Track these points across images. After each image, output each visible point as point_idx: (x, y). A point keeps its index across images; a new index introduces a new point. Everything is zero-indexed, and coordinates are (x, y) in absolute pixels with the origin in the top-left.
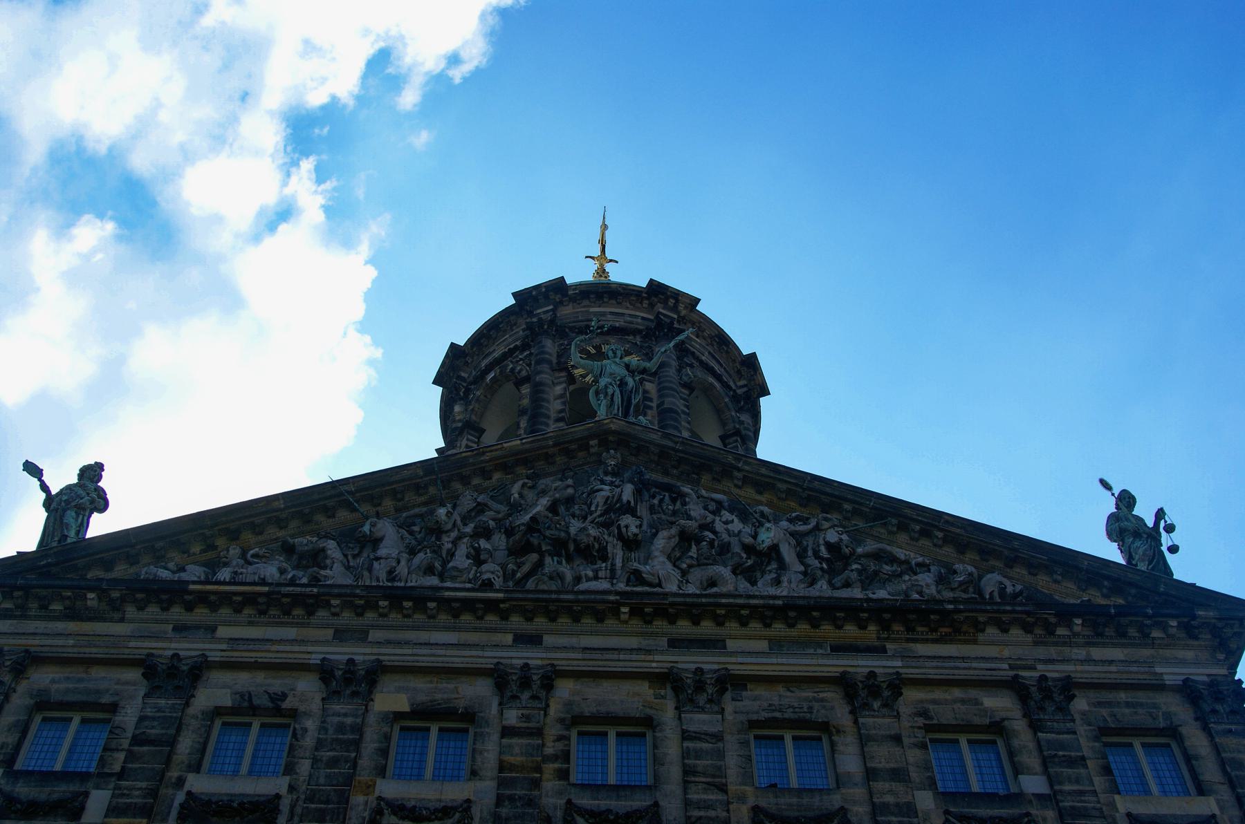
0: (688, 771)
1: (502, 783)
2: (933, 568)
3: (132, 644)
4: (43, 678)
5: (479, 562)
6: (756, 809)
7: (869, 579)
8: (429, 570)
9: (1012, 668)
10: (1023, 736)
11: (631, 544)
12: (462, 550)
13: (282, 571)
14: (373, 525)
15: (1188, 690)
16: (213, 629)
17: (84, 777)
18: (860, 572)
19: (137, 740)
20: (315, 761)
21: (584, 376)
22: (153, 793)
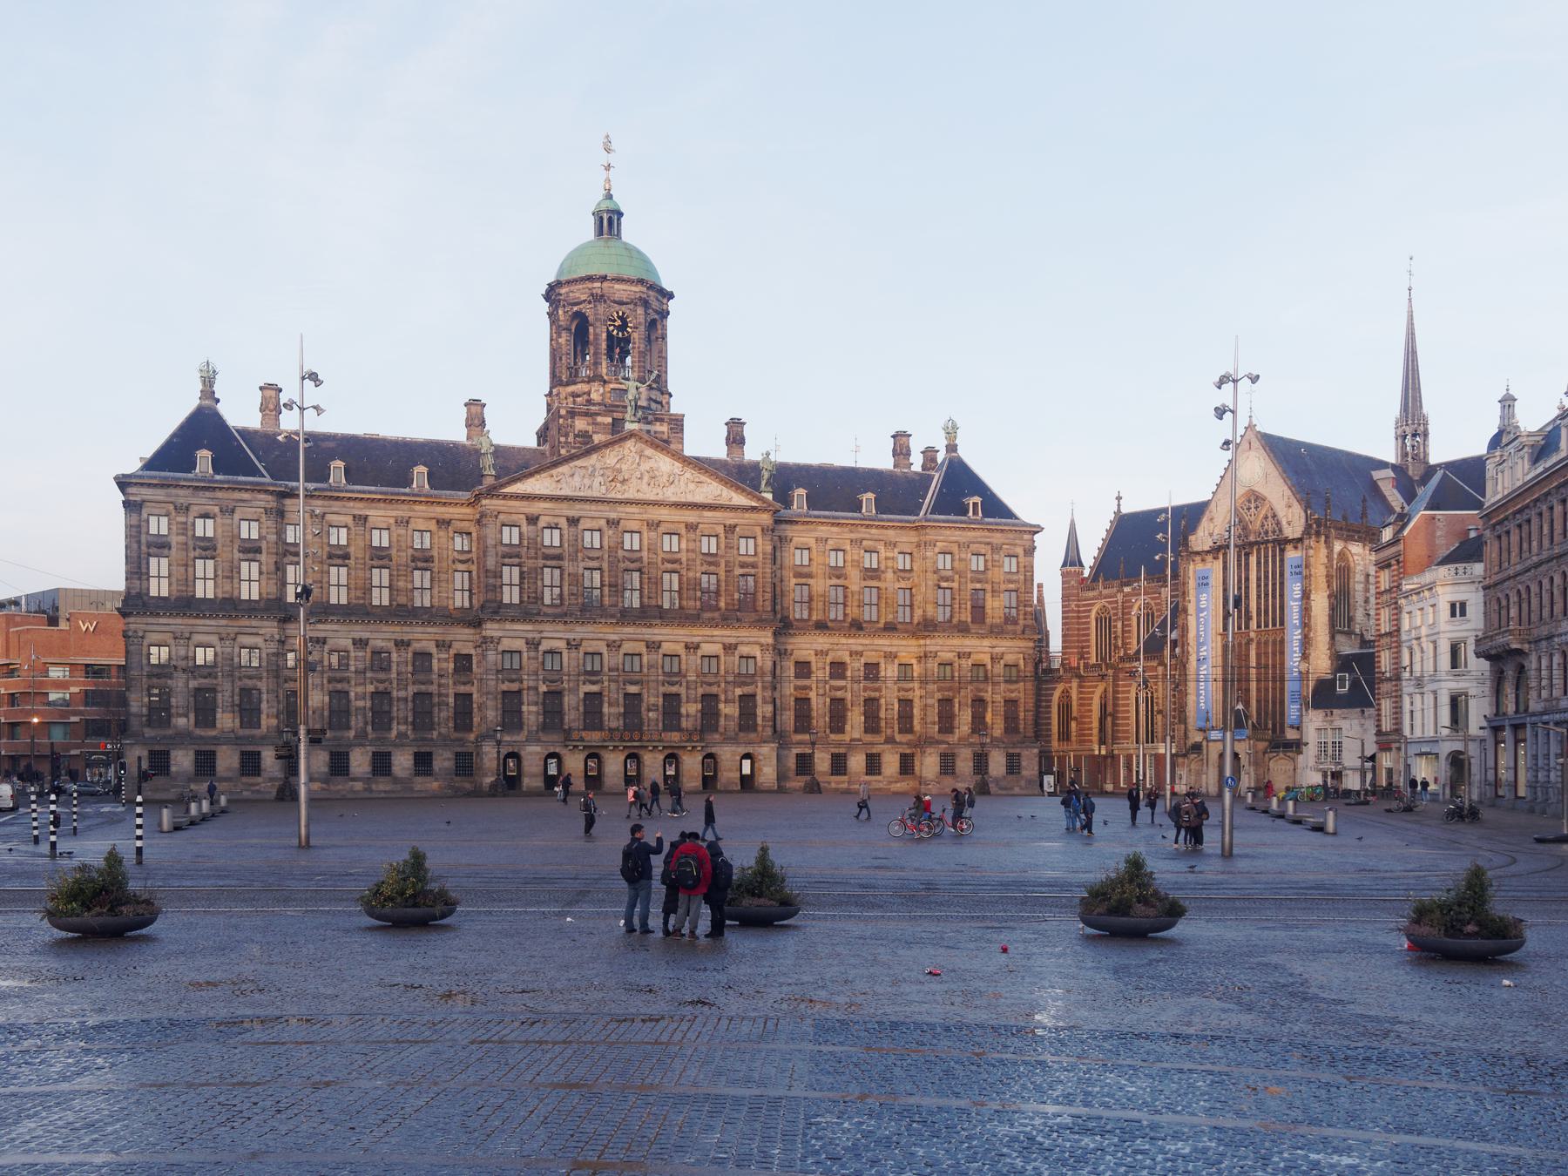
4: (501, 517)
10: (722, 539)
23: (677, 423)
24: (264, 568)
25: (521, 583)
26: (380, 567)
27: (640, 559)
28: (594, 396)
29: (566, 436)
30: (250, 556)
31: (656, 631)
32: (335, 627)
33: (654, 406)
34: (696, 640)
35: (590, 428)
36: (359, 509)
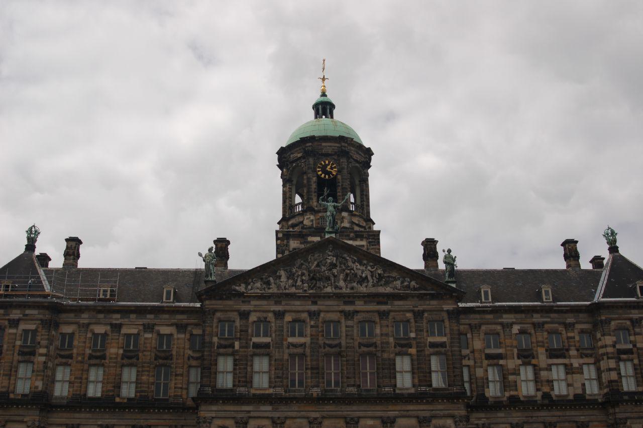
0: (347, 335)
1: (311, 339)
2: (401, 279)
3: (235, 307)
4: (218, 315)
5: (303, 283)
6: (359, 343)
7: (387, 283)
8: (293, 286)
9: (413, 307)
10: (413, 324)
11: (335, 276)
12: (299, 280)
13: (261, 285)
14: (279, 273)
15: (448, 311)
16: (250, 302)
17: (233, 339)
18: (385, 281)
19: (241, 331)
20: (276, 335)
21: (321, 175)
22: (247, 343)
23: (375, 238)
24: (36, 366)
25: (234, 369)
26: (131, 365)
27: (339, 345)
28: (306, 222)
29: (283, 253)
30: (27, 357)
31: (355, 408)
32: (88, 415)
33: (356, 228)
34: (391, 414)
35: (303, 246)
36: (116, 318)
